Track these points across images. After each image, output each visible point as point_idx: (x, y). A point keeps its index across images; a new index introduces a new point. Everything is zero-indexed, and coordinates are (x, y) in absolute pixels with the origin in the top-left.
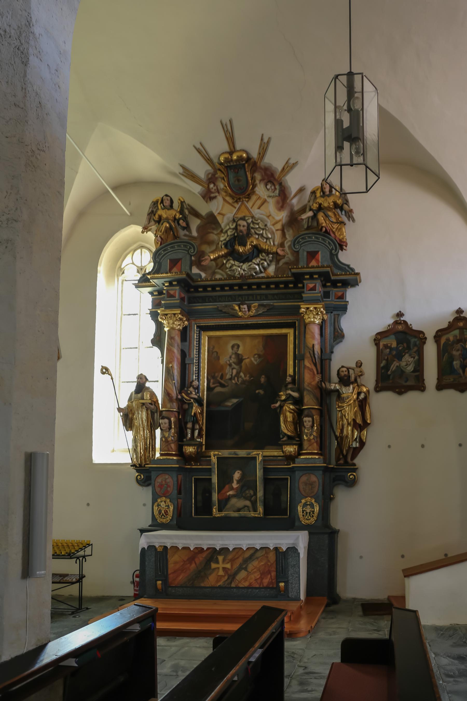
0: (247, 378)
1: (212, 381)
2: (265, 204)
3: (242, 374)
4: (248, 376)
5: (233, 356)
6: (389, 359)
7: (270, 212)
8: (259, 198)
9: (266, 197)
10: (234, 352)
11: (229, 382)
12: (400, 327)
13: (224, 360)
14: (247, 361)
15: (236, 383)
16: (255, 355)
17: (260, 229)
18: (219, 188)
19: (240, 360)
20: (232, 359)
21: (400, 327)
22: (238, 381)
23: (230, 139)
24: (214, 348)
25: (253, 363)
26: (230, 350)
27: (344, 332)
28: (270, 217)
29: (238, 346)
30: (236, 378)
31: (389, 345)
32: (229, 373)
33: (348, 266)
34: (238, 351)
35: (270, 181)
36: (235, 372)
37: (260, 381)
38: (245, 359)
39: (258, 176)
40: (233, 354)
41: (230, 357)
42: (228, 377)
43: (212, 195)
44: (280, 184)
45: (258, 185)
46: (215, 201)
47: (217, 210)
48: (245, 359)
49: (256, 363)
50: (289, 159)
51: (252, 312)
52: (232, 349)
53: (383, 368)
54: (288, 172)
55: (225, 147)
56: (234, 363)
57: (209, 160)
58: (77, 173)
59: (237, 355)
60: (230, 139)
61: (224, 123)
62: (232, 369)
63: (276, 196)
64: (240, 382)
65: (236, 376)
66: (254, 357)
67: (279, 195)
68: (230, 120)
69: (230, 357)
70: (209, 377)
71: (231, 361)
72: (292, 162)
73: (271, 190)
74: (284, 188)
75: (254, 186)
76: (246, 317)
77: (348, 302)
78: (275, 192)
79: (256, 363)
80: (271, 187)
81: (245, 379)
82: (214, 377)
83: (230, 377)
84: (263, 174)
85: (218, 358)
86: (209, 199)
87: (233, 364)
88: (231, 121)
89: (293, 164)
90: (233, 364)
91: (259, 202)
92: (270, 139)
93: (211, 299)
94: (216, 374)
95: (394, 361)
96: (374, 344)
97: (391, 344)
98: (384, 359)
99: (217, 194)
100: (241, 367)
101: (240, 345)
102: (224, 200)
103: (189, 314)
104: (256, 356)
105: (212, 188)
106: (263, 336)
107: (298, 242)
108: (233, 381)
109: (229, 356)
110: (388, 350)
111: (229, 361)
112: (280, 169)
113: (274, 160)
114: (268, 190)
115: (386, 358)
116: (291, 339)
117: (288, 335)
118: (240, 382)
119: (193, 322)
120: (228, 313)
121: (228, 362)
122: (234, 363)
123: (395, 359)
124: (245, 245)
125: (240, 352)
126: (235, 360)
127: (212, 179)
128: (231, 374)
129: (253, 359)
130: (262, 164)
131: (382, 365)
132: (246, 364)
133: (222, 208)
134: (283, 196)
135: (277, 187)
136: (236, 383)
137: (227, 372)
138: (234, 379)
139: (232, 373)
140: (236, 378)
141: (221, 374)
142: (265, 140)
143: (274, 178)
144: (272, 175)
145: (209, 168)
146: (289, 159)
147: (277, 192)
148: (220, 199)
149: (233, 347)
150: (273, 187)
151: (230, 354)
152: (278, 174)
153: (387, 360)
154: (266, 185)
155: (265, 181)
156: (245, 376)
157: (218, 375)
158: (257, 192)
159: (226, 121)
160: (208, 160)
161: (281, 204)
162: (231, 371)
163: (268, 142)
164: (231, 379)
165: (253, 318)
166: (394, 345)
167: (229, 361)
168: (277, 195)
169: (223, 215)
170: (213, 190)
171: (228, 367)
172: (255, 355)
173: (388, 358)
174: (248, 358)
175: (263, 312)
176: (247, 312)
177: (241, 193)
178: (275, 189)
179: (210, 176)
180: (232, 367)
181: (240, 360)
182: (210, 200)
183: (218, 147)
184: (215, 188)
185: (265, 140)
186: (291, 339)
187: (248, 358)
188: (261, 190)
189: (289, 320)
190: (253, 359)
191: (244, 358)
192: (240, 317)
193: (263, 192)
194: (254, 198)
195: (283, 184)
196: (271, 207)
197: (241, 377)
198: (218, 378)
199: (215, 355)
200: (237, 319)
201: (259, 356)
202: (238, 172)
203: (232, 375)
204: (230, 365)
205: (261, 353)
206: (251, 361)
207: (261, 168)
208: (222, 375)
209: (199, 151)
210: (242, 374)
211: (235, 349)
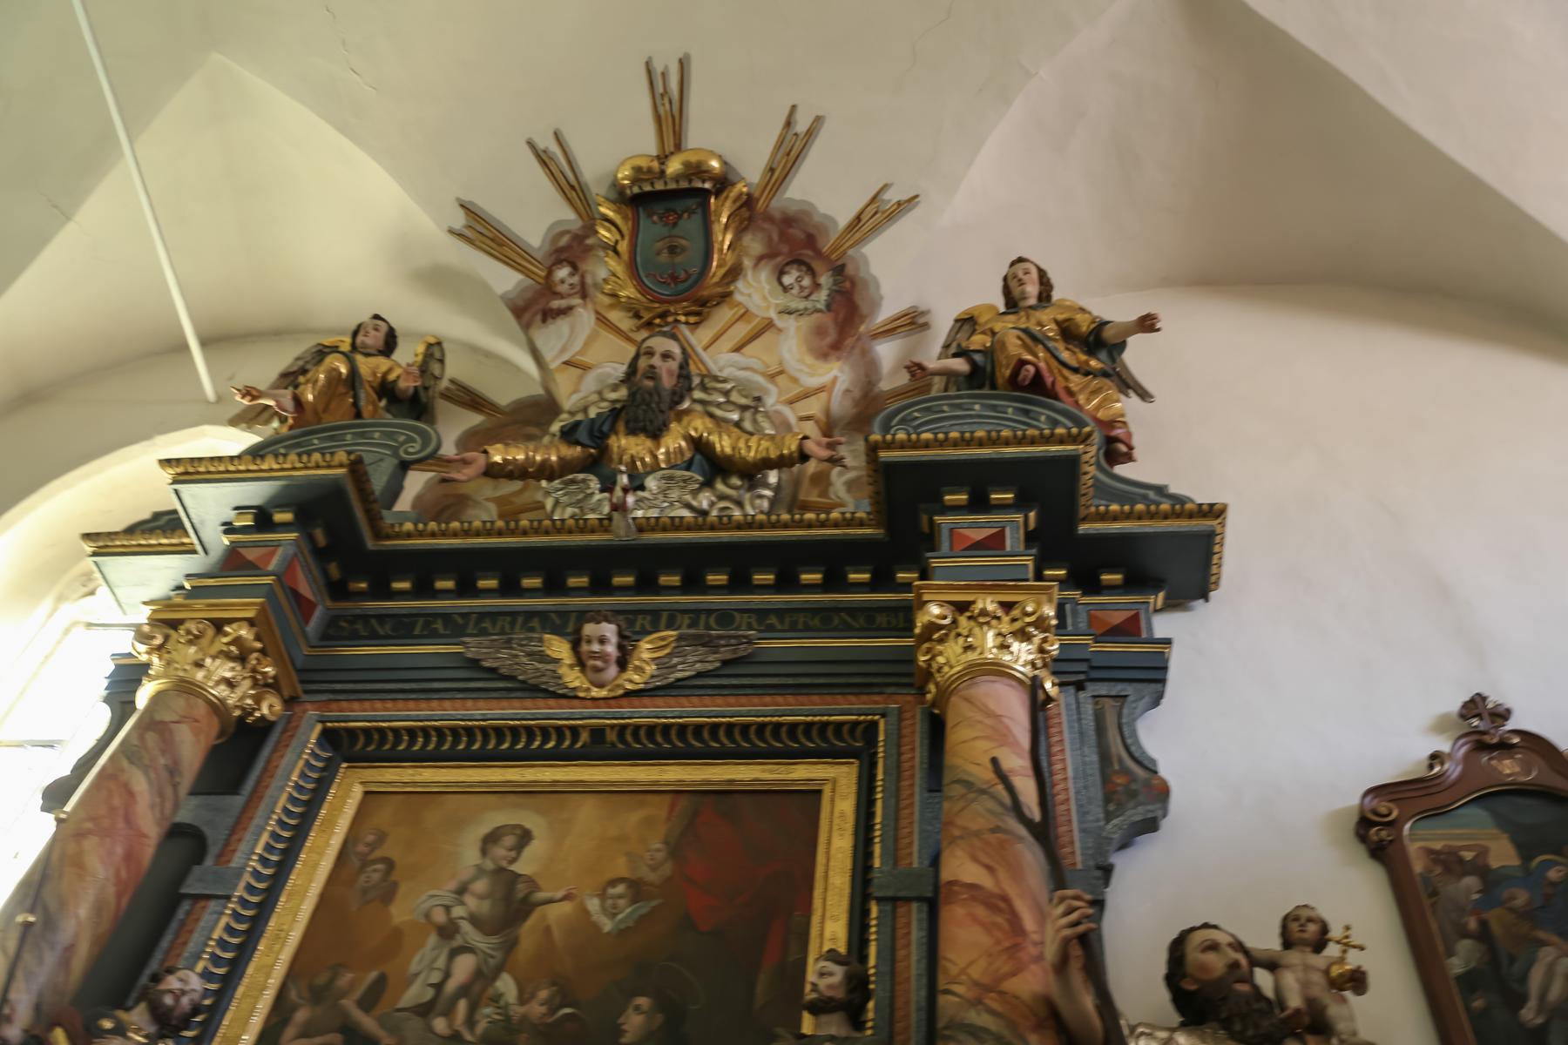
0: (536, 1009)
1: (301, 1016)
2: (767, 336)
3: (506, 986)
4: (544, 994)
5: (481, 886)
6: (1496, 929)
7: (781, 364)
8: (745, 315)
9: (772, 314)
10: (489, 865)
11: (416, 1023)
12: (1508, 767)
13: (413, 905)
14: (557, 913)
15: (456, 1036)
16: (613, 883)
17: (731, 407)
18: (589, 280)
19: (514, 903)
20: (471, 901)
21: (1508, 767)
22: (471, 1022)
23: (670, 120)
24: (381, 838)
25: (596, 927)
26: (470, 856)
27: (1164, 771)
28: (781, 379)
29: (525, 837)
30: (462, 1006)
31: (1468, 855)
32: (423, 970)
33: (1160, 490)
34: (513, 861)
35: (799, 262)
36: (464, 967)
37: (618, 1031)
38: (551, 901)
39: (754, 244)
40: (480, 871)
41: (462, 890)
42: (416, 993)
43: (556, 304)
44: (839, 270)
45: (750, 273)
46: (562, 326)
47: (563, 350)
48: (551, 901)
49: (607, 925)
50: (885, 187)
51: (639, 670)
52: (484, 852)
53: (1469, 982)
54: (876, 229)
55: (645, 143)
56: (474, 920)
57: (572, 189)
58: (68, 219)
59: (506, 879)
60: (670, 120)
61: (658, 68)
62: (454, 953)
63: (818, 311)
64: (481, 1026)
65: (464, 991)
66: (603, 896)
67: (829, 307)
68: (681, 62)
69: (462, 890)
70: (293, 995)
71: (458, 911)
72: (892, 196)
73: (795, 291)
74: (853, 283)
75: (734, 273)
76: (596, 693)
77: (1168, 642)
78: (813, 297)
79: (607, 925)
80: (799, 279)
81: (517, 1011)
82: (318, 995)
83: (429, 994)
84: (775, 237)
85: (388, 893)
86: (539, 317)
87: (466, 926)
88: (683, 64)
89: (899, 203)
90: (466, 926)
91: (741, 331)
92: (818, 121)
93: (439, 626)
94: (346, 978)
95: (1542, 943)
96: (1361, 851)
97: (1483, 852)
98: (1464, 934)
99: (576, 301)
100: (510, 946)
101: (536, 833)
102: (602, 319)
103: (307, 680)
104: (620, 889)
105: (563, 282)
106: (677, 792)
107: (902, 421)
108: (440, 1024)
109: (453, 885)
110: (1471, 882)
111: (447, 908)
112: (843, 220)
113: (825, 192)
114: (786, 289)
115: (1472, 924)
116: (840, 810)
117: (827, 790)
118: (481, 1026)
119: (312, 713)
120: (512, 678)
121: (439, 917)
122: (474, 920)
123: (1541, 935)
124: (656, 434)
125: (517, 868)
126: (484, 908)
127: (571, 250)
128: (435, 978)
129: (593, 905)
130: (776, 204)
131: (1457, 965)
132: (547, 930)
133: (586, 345)
134: (845, 313)
135: (825, 279)
136: (456, 1036)
137: (414, 967)
138: (448, 1012)
139: (447, 975)
140: (462, 1006)
141: (373, 975)
142: (801, 126)
143: (818, 254)
144: (811, 241)
145: (567, 215)
146: (885, 187)
147: (822, 296)
148: (585, 318)
149: (491, 839)
150: (806, 282)
151: (465, 875)
152: (833, 237)
153: (1484, 935)
154: (781, 273)
155: (779, 259)
156: (523, 1000)
157: (354, 982)
158: (738, 297)
159: (667, 61)
160: (572, 187)
161: (832, 337)
162: (441, 962)
163: (811, 133)
164: (425, 1010)
165: (635, 701)
166: (1503, 854)
167: (447, 908)
168: (821, 306)
169: (585, 368)
170: (564, 288)
171: (433, 939)
172: (613, 883)
173: (1484, 924)
174: (566, 898)
175: (700, 675)
176: (613, 670)
177: (680, 291)
178: (817, 286)
179: (564, 241)
180: (458, 941)
181: (514, 903)
182: (544, 321)
183: (616, 145)
184: (575, 280)
185: (801, 126)
186: (840, 810)
187: (566, 898)
188: (757, 291)
189: (842, 710)
190: (593, 905)
191: (541, 895)
192: (571, 696)
193: (765, 298)
194: (723, 315)
195: (850, 270)
196: (792, 346)
197: (496, 999)
198: (349, 1004)
199: (376, 877)
200: (552, 702)
201: (637, 889)
202: (675, 225)
203: (438, 987)
204: (447, 931)
205: (651, 877)
206: (586, 912)
207: (769, 218)
208: (380, 984)
209: (543, 159)
210: (506, 986)
211: (500, 851)
